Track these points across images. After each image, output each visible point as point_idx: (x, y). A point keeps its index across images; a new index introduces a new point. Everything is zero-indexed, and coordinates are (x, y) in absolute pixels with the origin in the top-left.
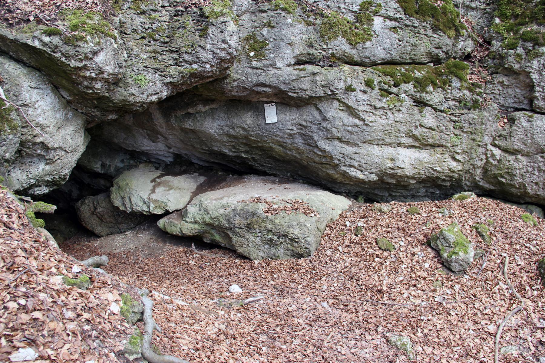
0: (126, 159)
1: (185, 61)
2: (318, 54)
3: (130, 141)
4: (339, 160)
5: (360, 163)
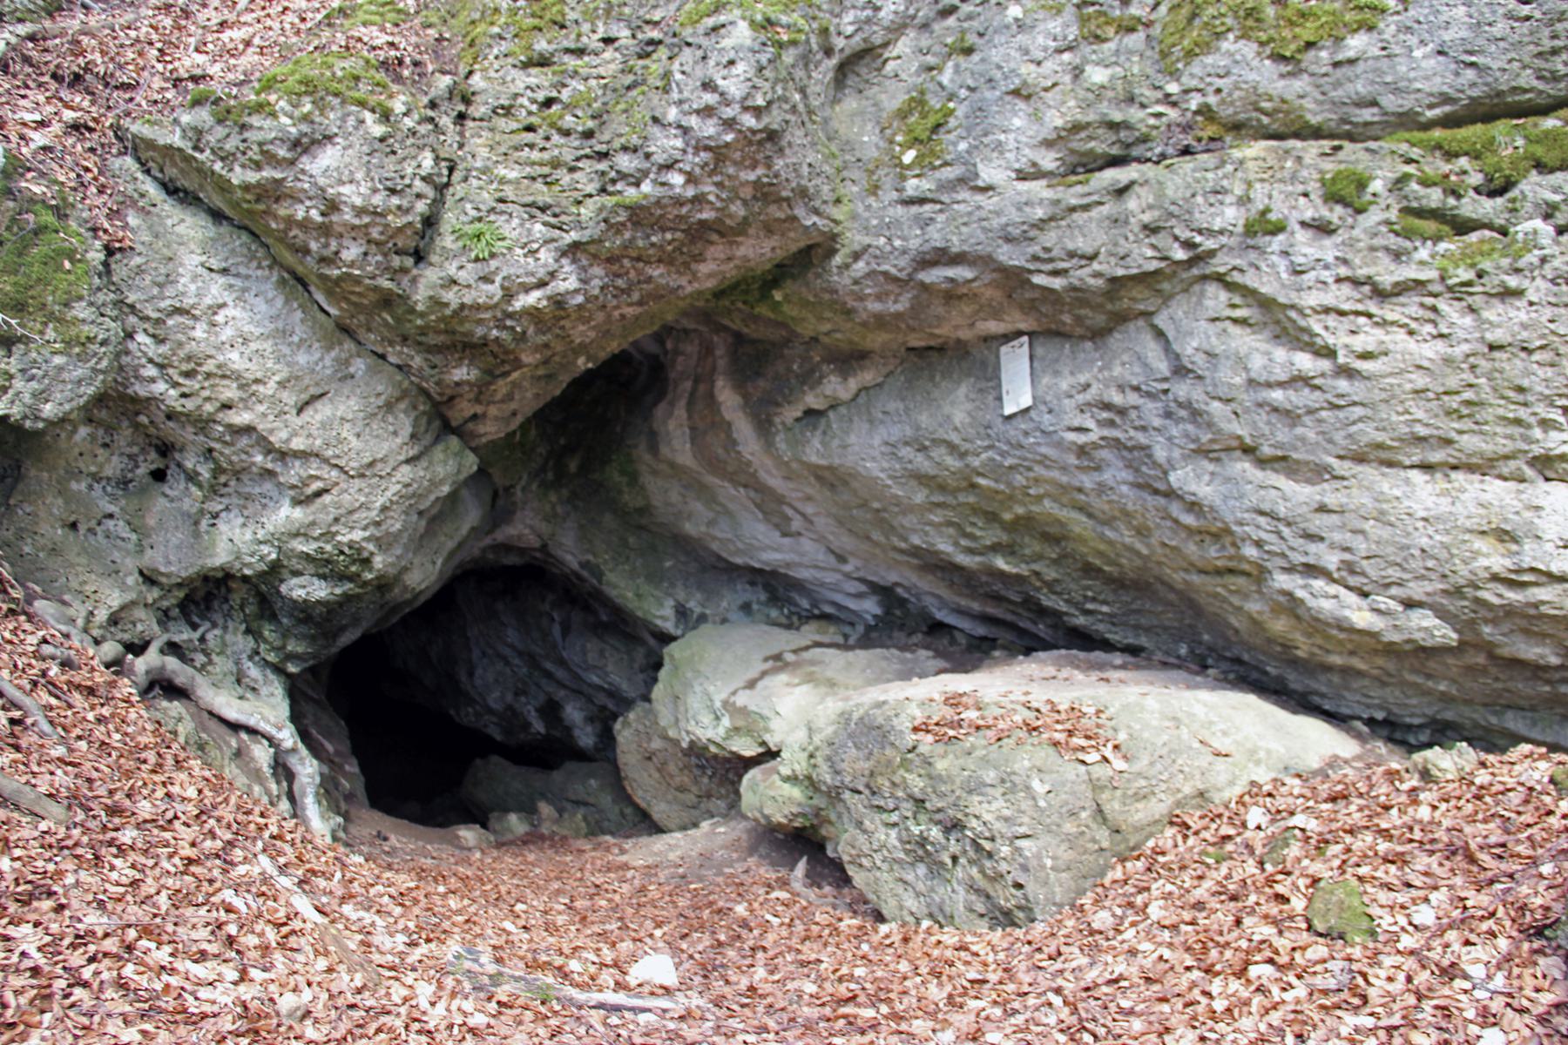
0: (759, 602)
1: (622, 176)
2: (1152, 121)
3: (722, 531)
4: (1259, 544)
5: (1347, 556)
